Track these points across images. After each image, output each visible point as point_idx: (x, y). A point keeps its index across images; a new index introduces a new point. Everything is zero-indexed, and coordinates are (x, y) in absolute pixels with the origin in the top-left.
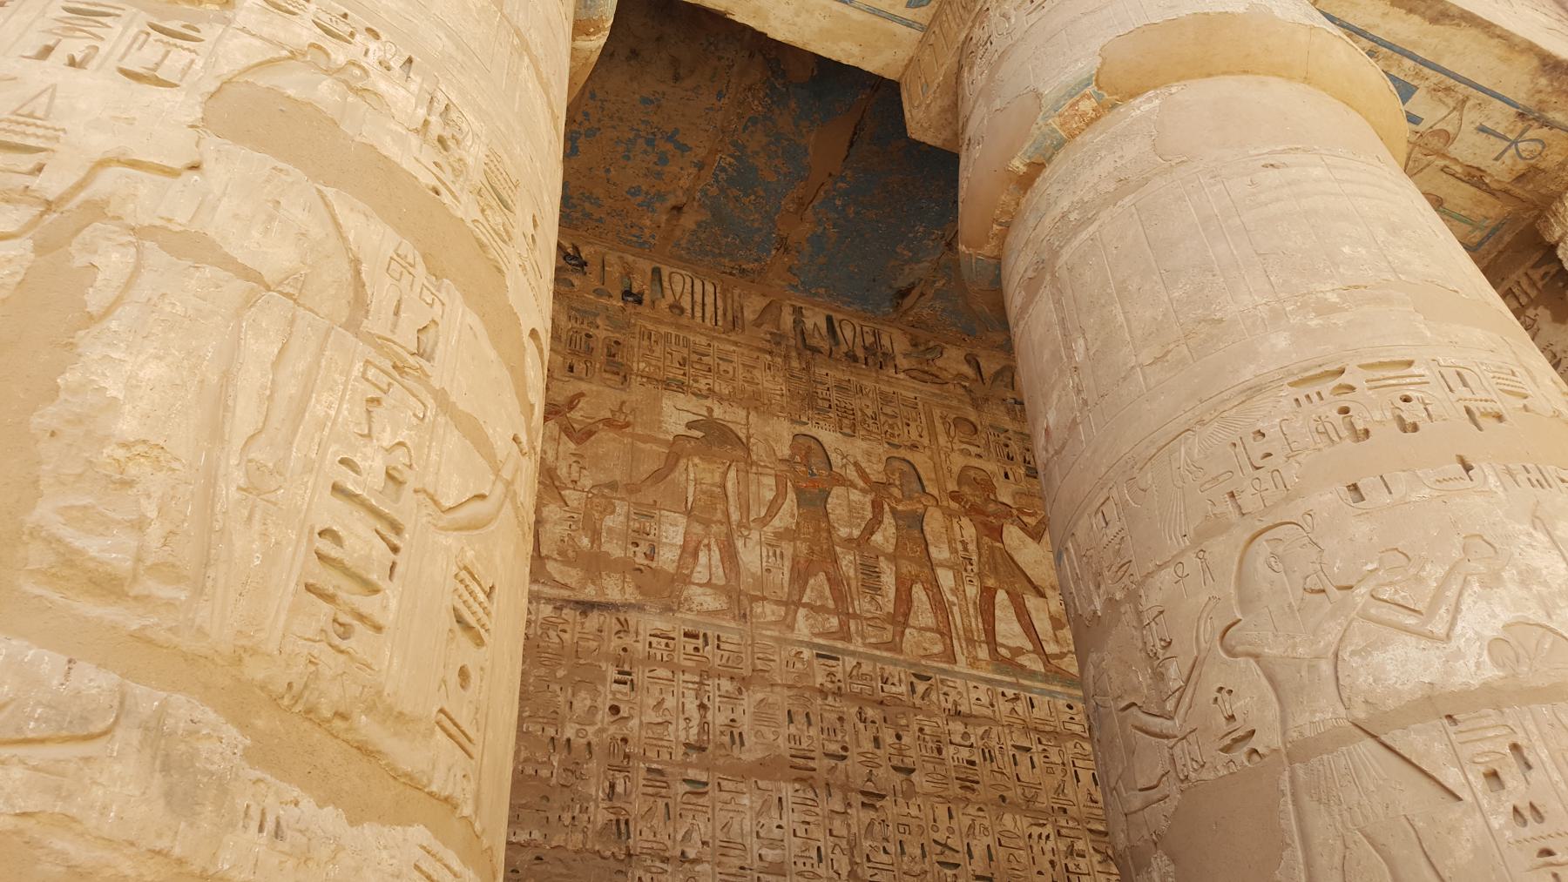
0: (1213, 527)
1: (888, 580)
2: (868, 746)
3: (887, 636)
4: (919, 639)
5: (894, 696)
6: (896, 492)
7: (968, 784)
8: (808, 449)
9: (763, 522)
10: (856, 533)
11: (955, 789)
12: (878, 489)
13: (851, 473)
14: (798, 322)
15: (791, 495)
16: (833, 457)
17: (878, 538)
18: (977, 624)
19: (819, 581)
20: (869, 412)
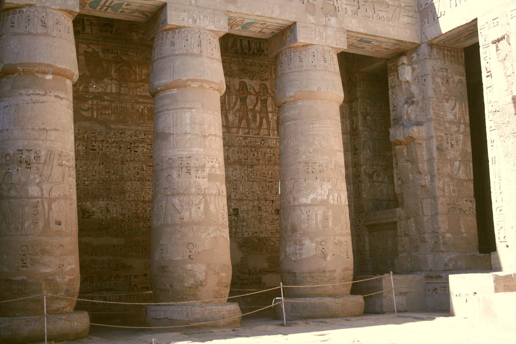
0: (292, 179)
1: (258, 118)
2: (252, 156)
3: (257, 132)
4: (264, 132)
5: (258, 145)
6: (261, 94)
7: (270, 161)
8: (243, 85)
9: (233, 108)
10: (252, 107)
11: (267, 162)
12: (257, 94)
13: (252, 91)
14: (241, 44)
15: (239, 100)
16: (249, 87)
17: (257, 108)
18: (275, 126)
19: (244, 121)
20: (257, 71)
